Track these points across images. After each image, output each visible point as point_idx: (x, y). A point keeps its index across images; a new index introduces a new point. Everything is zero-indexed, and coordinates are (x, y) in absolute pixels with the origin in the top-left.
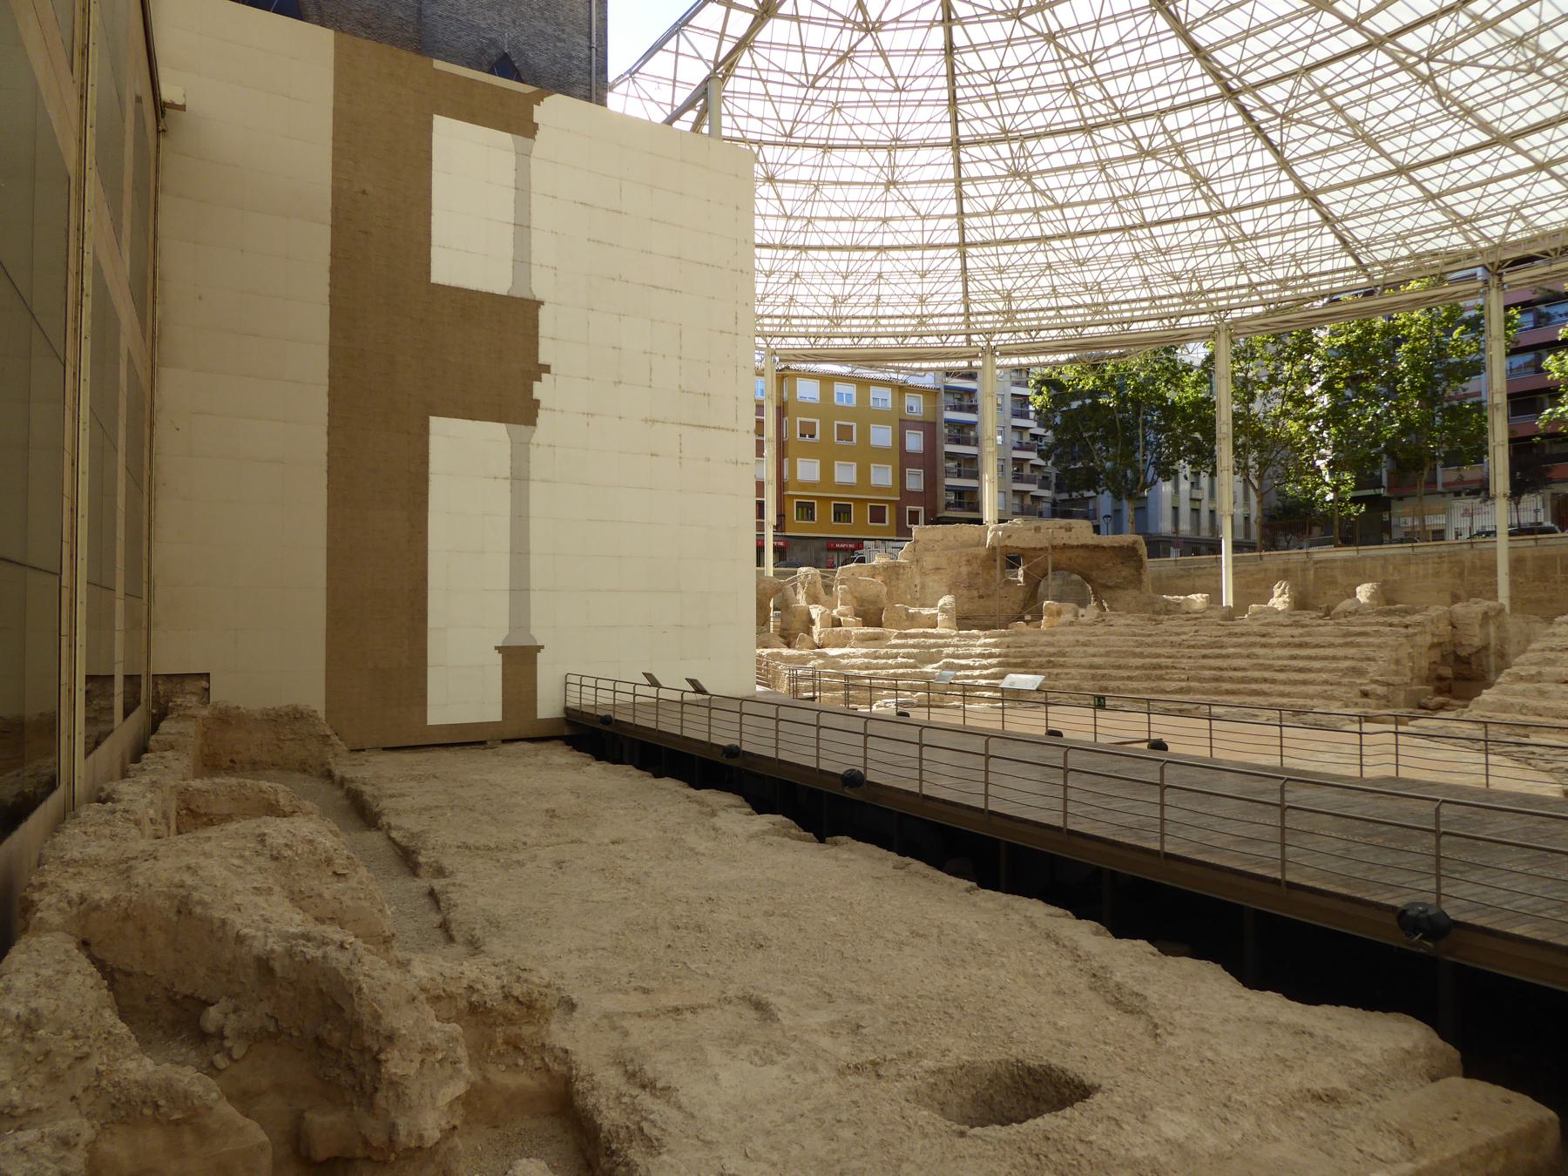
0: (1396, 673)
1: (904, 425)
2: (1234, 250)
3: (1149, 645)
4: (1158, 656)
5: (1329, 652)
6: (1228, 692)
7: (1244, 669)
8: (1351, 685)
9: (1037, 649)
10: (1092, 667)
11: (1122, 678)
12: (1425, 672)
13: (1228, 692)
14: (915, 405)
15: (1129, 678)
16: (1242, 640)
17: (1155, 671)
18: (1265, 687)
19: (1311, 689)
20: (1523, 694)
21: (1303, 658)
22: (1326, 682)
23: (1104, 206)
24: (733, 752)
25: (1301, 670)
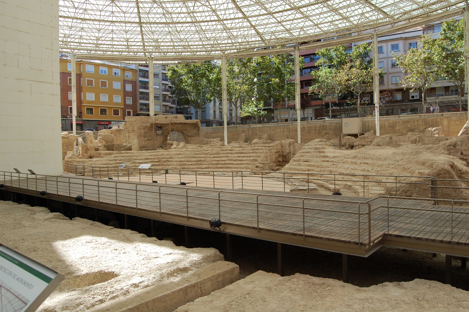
0: (266, 160)
1: (125, 82)
2: (226, 32)
3: (198, 154)
4: (201, 157)
5: (248, 155)
6: (220, 168)
7: (225, 161)
9: (163, 156)
10: (180, 161)
11: (189, 165)
12: (274, 160)
13: (220, 168)
14: (129, 75)
15: (191, 165)
16: (225, 152)
17: (199, 162)
18: (230, 166)
19: (243, 166)
20: (295, 165)
21: (241, 157)
22: (247, 164)
23: (186, 15)
24: (43, 193)
25: (241, 160)
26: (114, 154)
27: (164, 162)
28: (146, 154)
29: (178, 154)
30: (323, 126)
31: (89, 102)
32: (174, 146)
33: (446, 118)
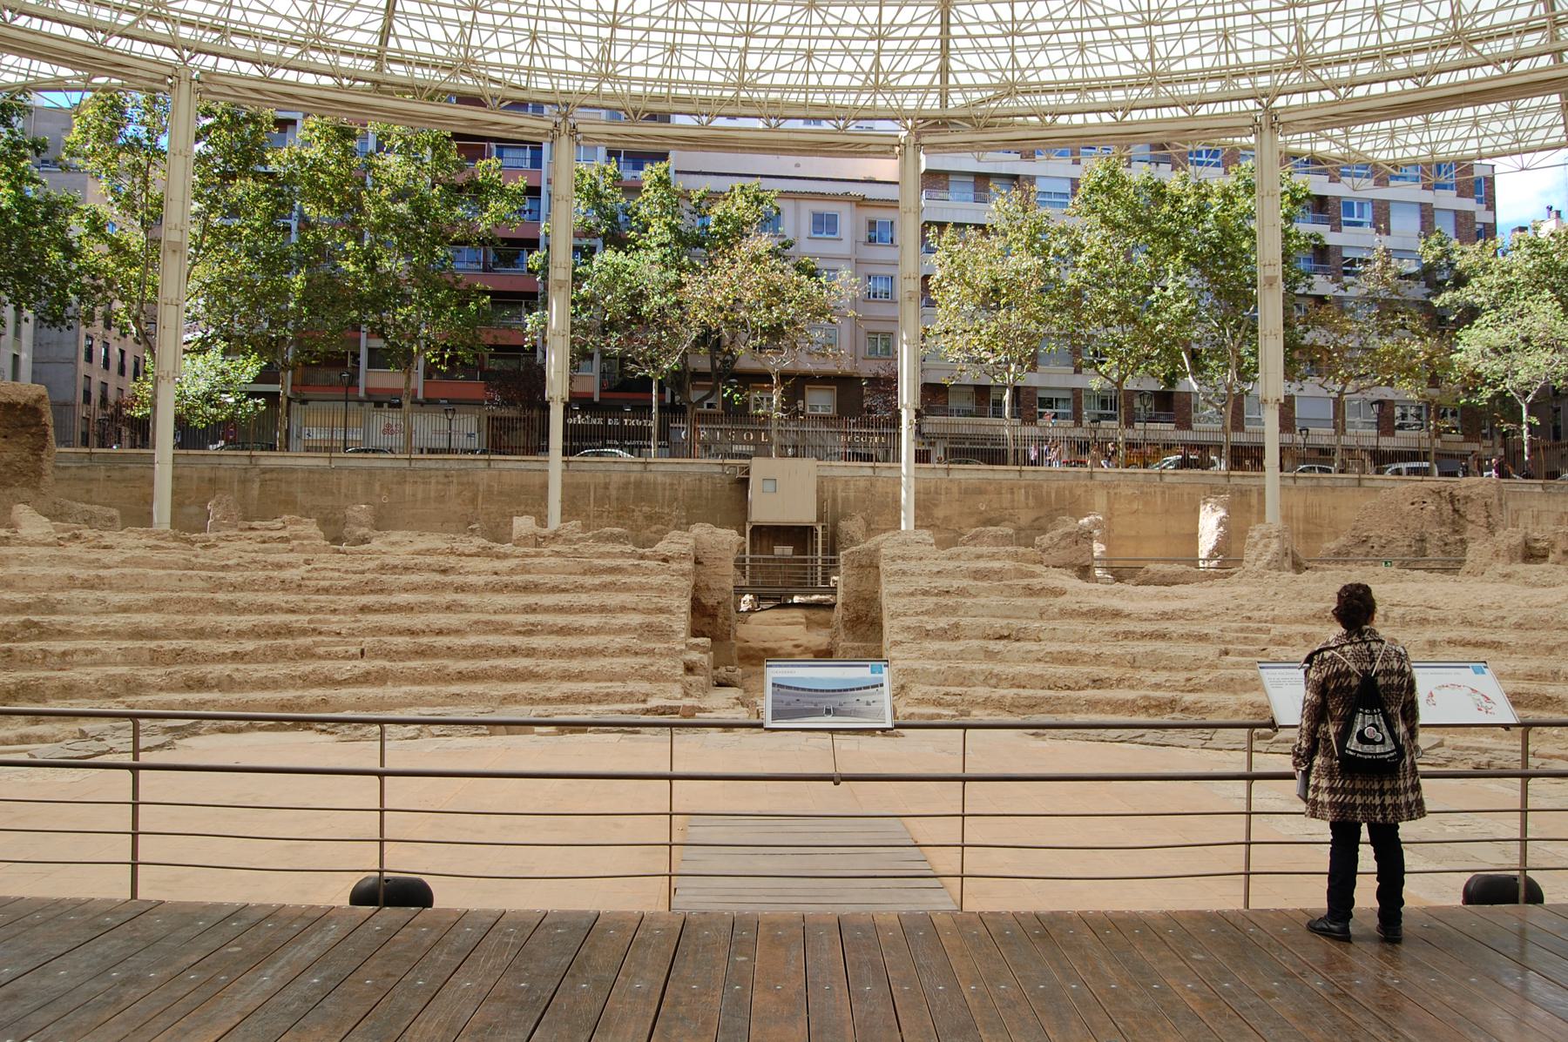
3: (235, 587)
4: (270, 609)
5: (584, 599)
6: (462, 677)
7: (457, 632)
8: (671, 653)
10: (138, 634)
11: (221, 658)
13: (462, 677)
15: (237, 656)
16: (416, 578)
21: (547, 610)
22: (626, 651)
30: (638, 484)
33: (1105, 485)
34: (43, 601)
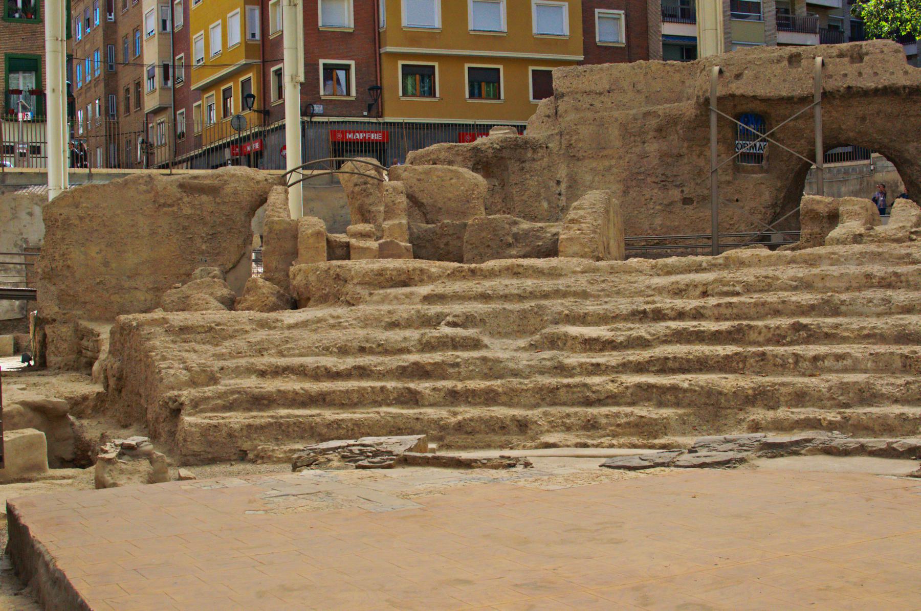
9: (771, 298)
26: (432, 279)
27: (778, 338)
28: (643, 281)
29: (886, 283)
31: (415, 37)
32: (850, 226)
34: (827, 302)
